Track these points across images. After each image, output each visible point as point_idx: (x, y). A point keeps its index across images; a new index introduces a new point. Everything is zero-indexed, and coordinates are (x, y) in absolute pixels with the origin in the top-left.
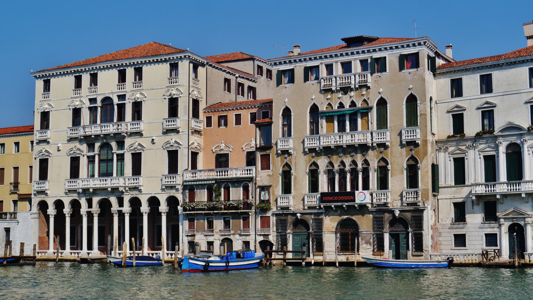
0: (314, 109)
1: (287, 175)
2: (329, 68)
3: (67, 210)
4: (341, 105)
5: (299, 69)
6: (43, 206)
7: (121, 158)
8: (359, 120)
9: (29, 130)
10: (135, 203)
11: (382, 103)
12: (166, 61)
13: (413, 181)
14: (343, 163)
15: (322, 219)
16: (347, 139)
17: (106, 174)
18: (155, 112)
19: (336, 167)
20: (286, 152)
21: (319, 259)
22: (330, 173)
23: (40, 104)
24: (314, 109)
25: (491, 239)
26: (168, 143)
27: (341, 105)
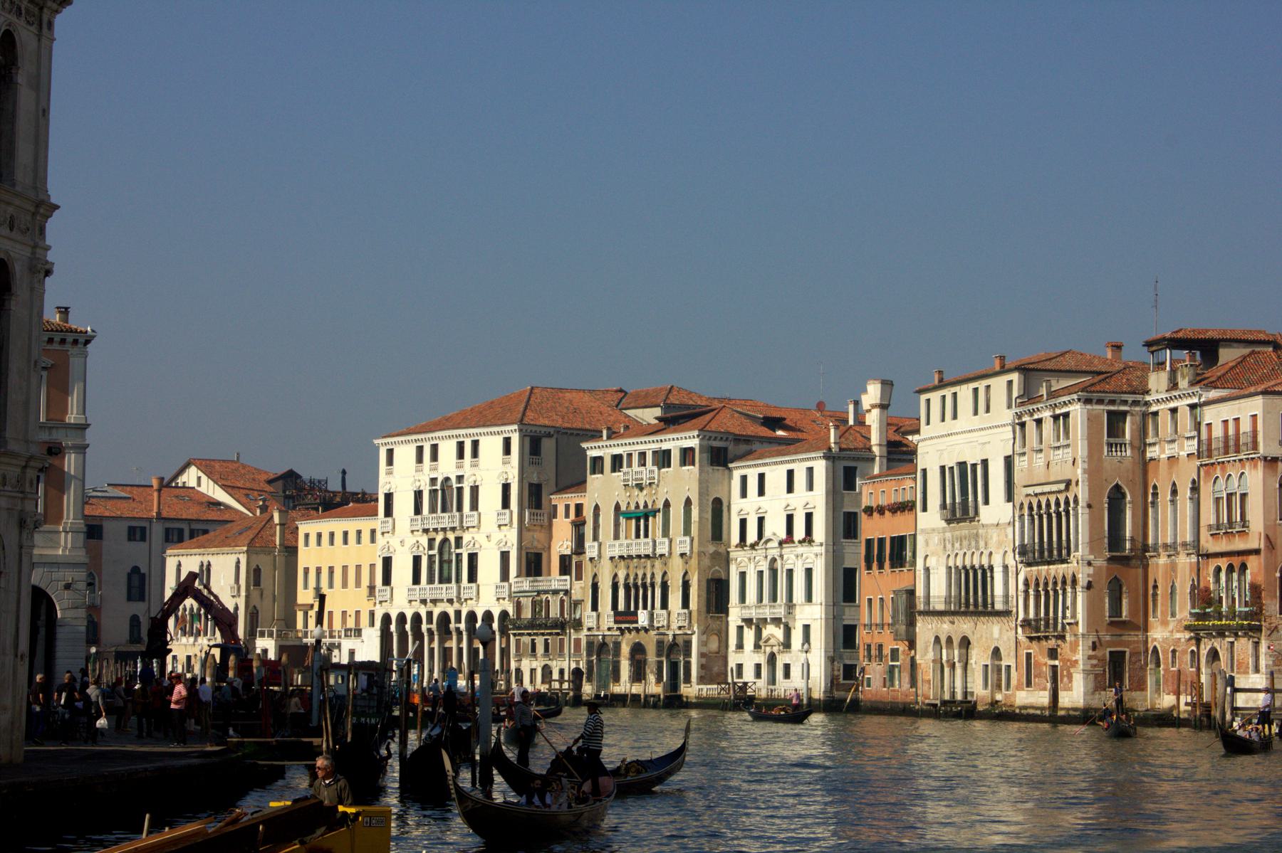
0: (617, 507)
1: (595, 587)
2: (630, 455)
4: (637, 507)
6: (386, 619)
7: (459, 556)
10: (472, 616)
11: (667, 504)
17: (445, 579)
18: (490, 499)
19: (631, 581)
20: (591, 559)
22: (627, 587)
24: (617, 507)
26: (500, 542)
27: (637, 507)
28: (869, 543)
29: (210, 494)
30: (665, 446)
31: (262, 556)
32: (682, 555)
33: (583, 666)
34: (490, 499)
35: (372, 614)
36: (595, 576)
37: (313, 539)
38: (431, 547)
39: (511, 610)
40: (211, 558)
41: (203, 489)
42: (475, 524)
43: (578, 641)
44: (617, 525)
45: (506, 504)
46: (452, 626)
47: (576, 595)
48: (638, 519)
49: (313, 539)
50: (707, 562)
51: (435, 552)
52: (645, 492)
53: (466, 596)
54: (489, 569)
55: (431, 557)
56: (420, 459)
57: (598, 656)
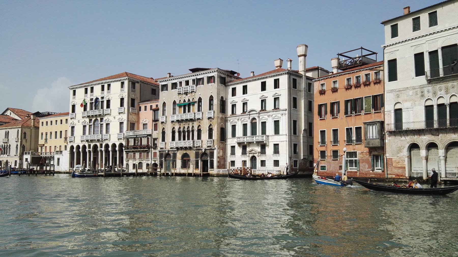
0: (174, 103)
1: (164, 133)
2: (181, 83)
3: (81, 150)
4: (185, 101)
5: (169, 84)
6: (72, 147)
7: (102, 125)
8: (191, 107)
9: (67, 114)
10: (107, 146)
12: (119, 81)
13: (210, 136)
14: (184, 127)
15: (176, 153)
16: (184, 117)
18: (115, 104)
19: (182, 129)
20: (162, 123)
21: (173, 171)
22: (179, 132)
23: (72, 101)
25: (244, 162)
26: (119, 119)
27: (185, 101)
28: (320, 106)
29: (14, 117)
30: (199, 77)
31: (27, 129)
32: (209, 118)
33: (158, 162)
34: (115, 104)
35: (66, 146)
36: (164, 128)
37: (45, 124)
38: (90, 123)
39: (124, 143)
40: (9, 130)
41: (12, 116)
42: (109, 113)
43: (155, 153)
44: (174, 109)
45: (122, 105)
46: (99, 149)
47: (154, 136)
48: (185, 106)
49: (45, 124)
50: (219, 121)
51: (92, 124)
52: (189, 95)
53: (105, 138)
54: (114, 128)
55: (90, 125)
56: (86, 92)
57: (165, 158)
